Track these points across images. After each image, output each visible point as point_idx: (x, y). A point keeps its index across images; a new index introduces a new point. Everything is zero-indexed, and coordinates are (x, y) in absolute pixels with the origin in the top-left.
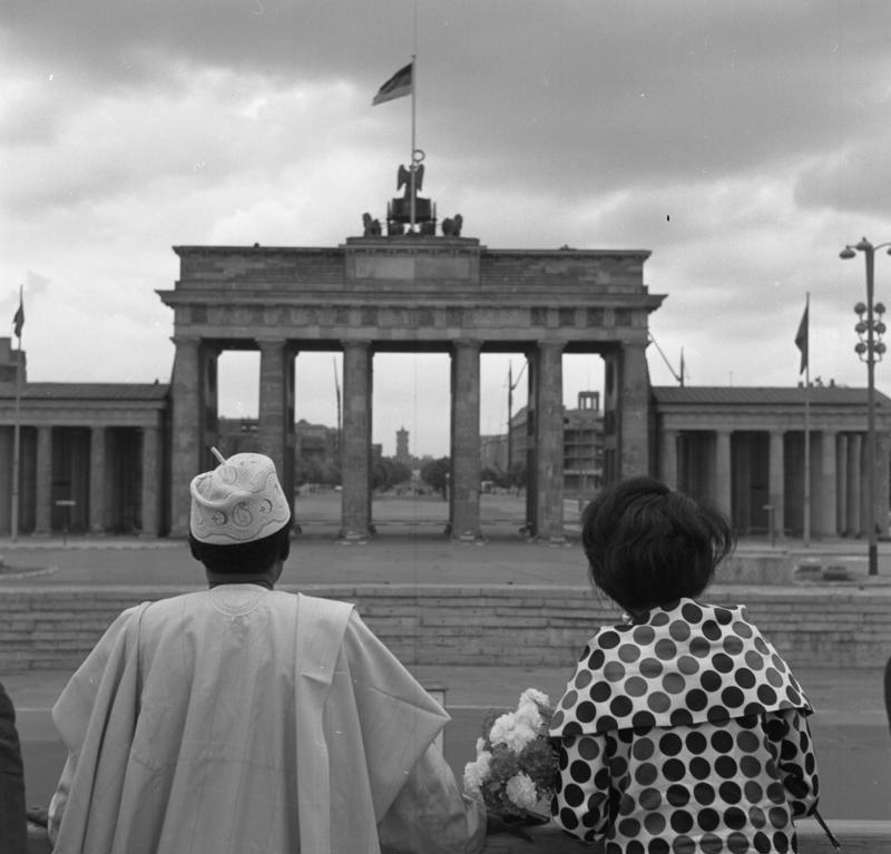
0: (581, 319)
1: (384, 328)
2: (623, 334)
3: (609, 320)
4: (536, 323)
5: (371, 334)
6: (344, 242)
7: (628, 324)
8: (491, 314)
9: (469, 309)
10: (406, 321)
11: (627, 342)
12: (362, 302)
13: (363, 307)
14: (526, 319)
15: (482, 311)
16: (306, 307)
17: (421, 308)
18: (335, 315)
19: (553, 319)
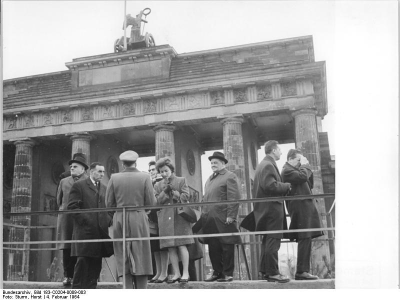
0: (252, 95)
1: (98, 121)
2: (290, 103)
3: (277, 92)
4: (215, 104)
5: (88, 127)
6: (72, 61)
7: (294, 94)
8: (178, 100)
9: (160, 98)
10: (114, 115)
11: (294, 109)
12: (78, 102)
13: (80, 107)
14: (207, 101)
15: (172, 99)
16: (40, 112)
17: (122, 102)
18: (63, 116)
19: (229, 98)
